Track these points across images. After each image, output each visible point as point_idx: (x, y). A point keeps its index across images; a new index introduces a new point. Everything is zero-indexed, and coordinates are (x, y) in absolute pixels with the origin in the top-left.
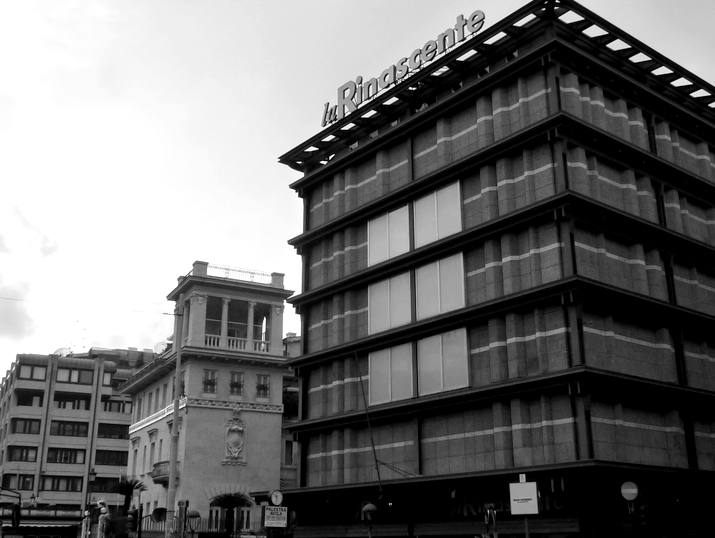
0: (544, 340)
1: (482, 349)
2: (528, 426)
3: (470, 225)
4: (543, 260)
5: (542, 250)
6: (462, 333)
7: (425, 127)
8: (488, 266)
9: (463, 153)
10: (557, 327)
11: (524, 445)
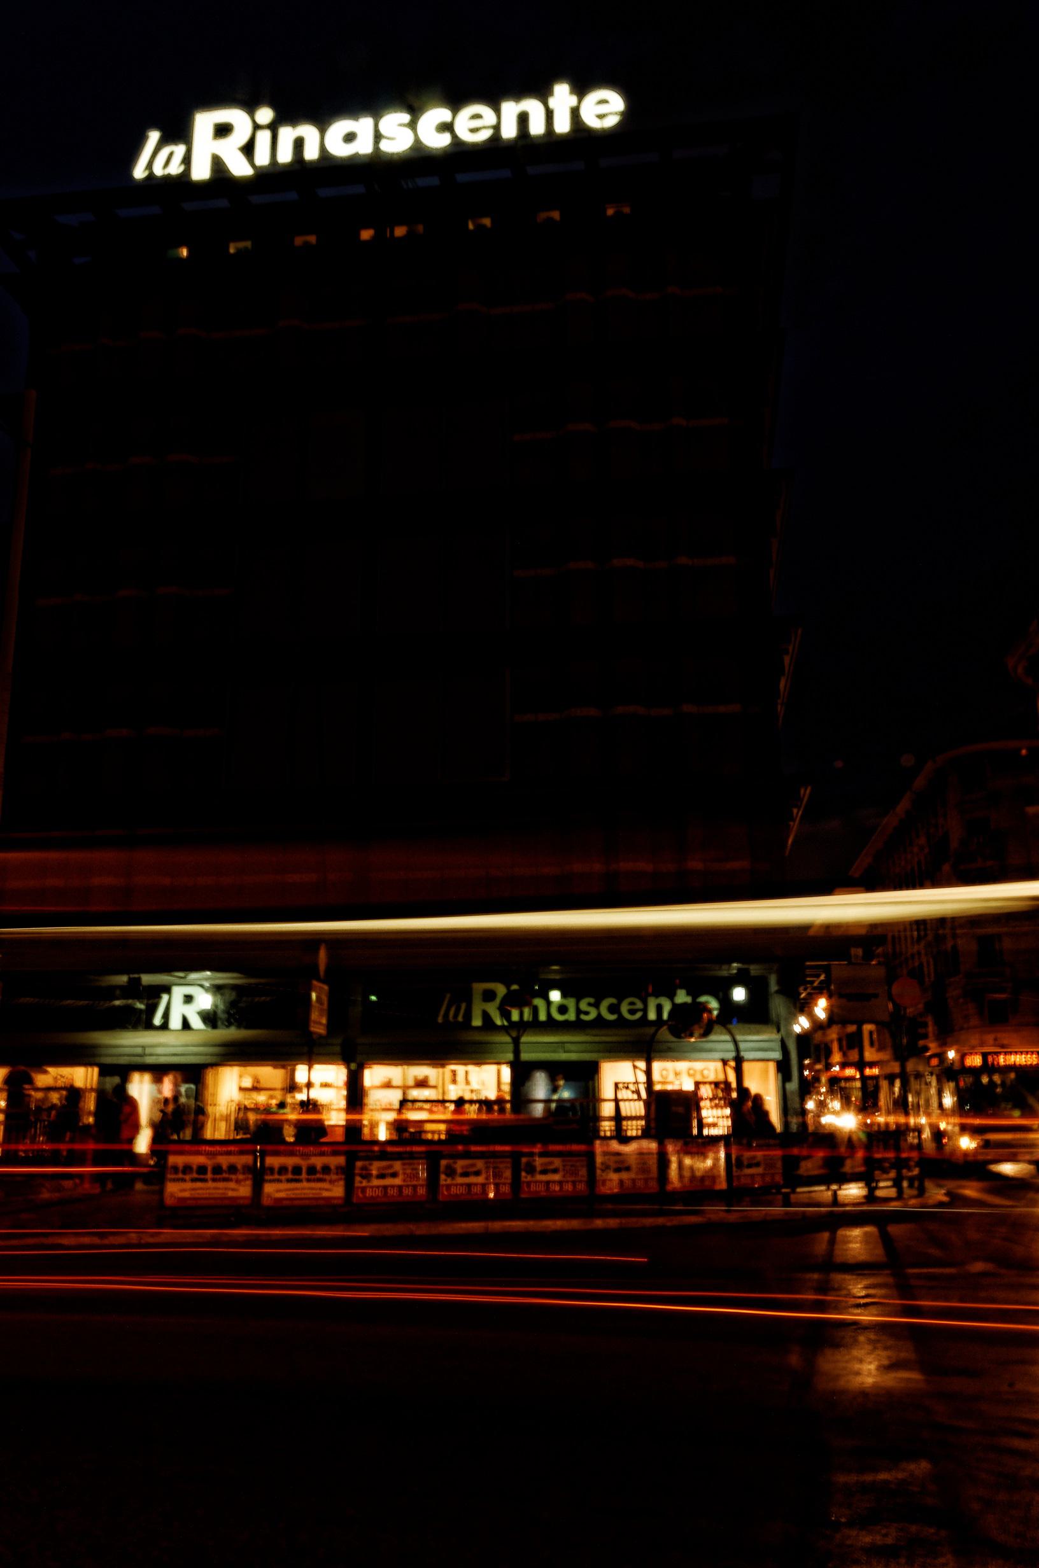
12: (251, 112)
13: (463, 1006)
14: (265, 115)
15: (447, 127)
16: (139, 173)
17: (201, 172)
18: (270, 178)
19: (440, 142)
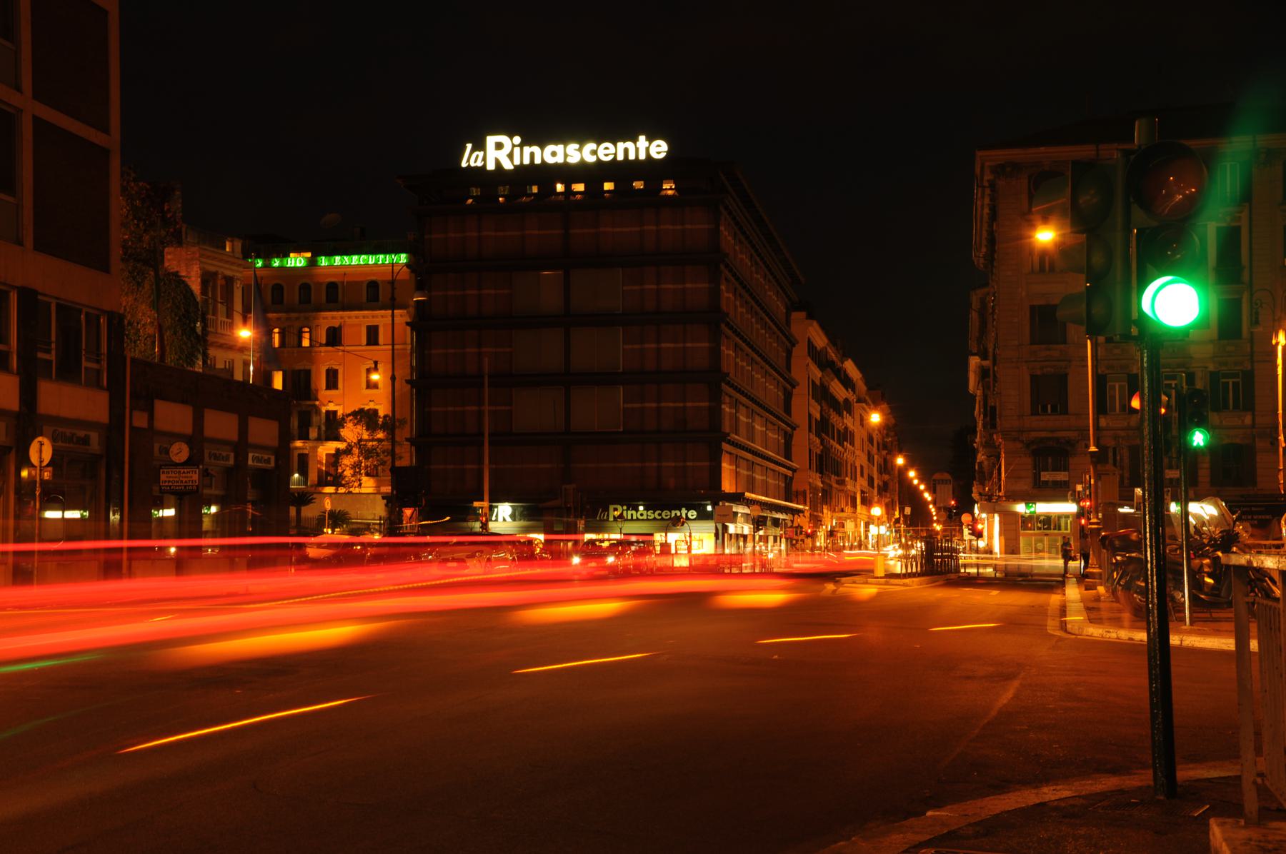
12: (511, 137)
14: (517, 140)
15: (594, 152)
16: (464, 164)
17: (491, 166)
18: (520, 169)
19: (591, 159)
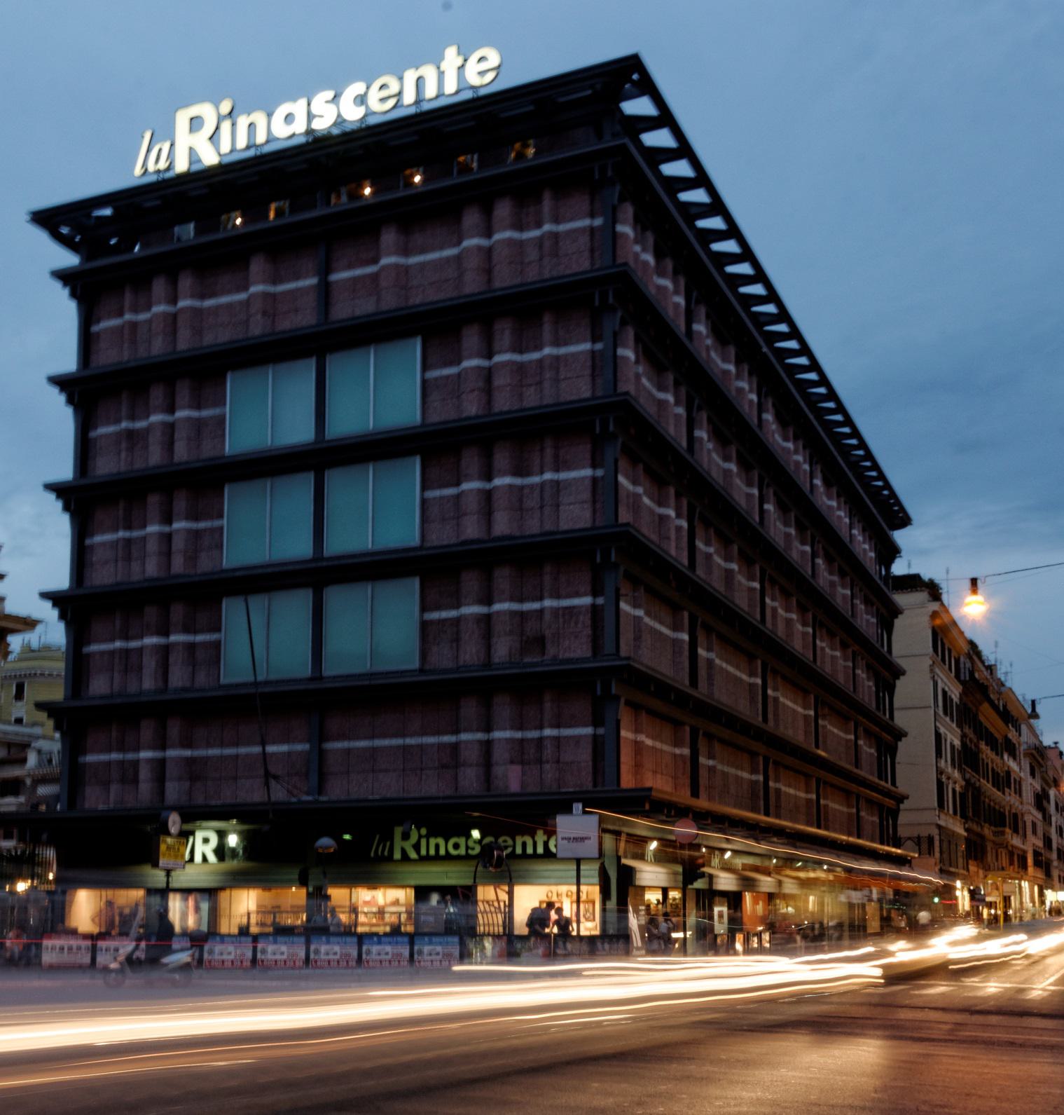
0: (555, 611)
1: (445, 614)
2: (518, 735)
3: (434, 418)
4: (567, 489)
5: (563, 476)
6: (415, 583)
7: (360, 229)
8: (466, 486)
9: (424, 295)
10: (577, 594)
11: (512, 762)
13: (388, 844)
